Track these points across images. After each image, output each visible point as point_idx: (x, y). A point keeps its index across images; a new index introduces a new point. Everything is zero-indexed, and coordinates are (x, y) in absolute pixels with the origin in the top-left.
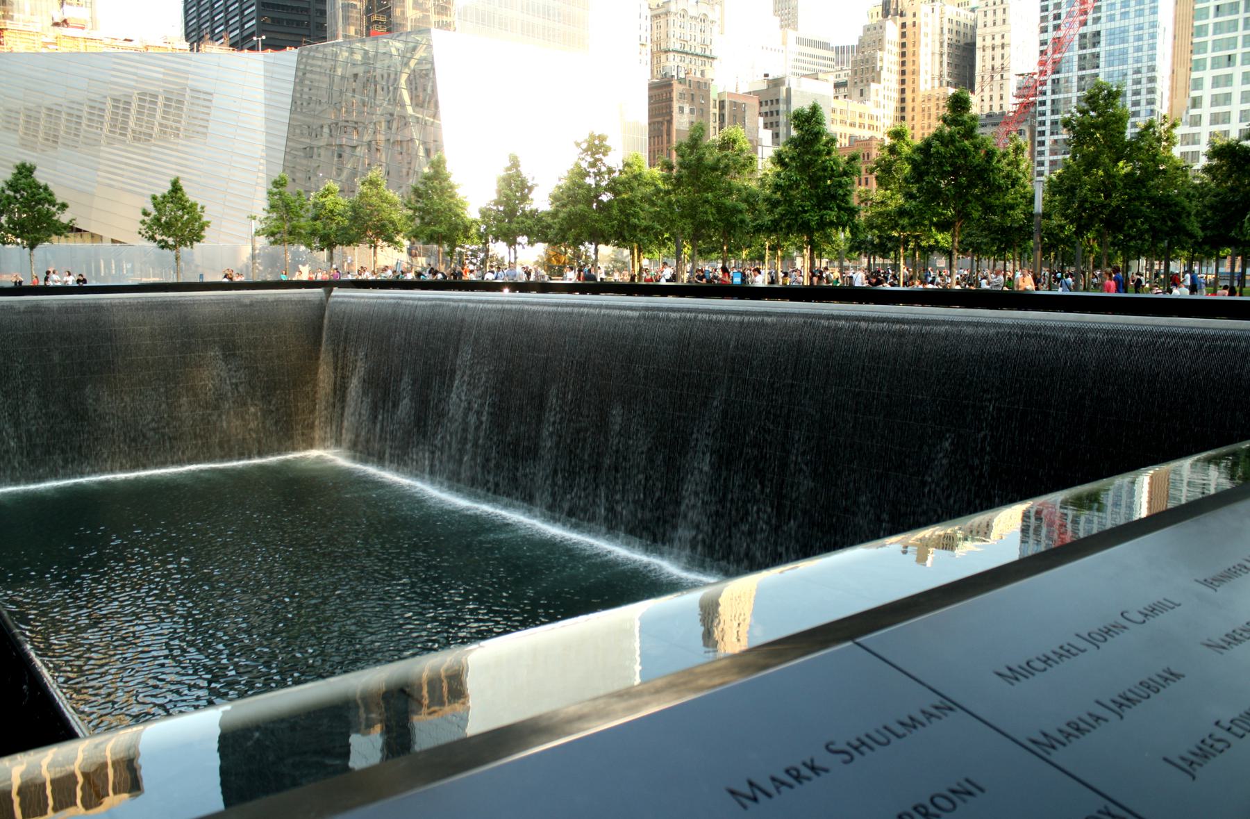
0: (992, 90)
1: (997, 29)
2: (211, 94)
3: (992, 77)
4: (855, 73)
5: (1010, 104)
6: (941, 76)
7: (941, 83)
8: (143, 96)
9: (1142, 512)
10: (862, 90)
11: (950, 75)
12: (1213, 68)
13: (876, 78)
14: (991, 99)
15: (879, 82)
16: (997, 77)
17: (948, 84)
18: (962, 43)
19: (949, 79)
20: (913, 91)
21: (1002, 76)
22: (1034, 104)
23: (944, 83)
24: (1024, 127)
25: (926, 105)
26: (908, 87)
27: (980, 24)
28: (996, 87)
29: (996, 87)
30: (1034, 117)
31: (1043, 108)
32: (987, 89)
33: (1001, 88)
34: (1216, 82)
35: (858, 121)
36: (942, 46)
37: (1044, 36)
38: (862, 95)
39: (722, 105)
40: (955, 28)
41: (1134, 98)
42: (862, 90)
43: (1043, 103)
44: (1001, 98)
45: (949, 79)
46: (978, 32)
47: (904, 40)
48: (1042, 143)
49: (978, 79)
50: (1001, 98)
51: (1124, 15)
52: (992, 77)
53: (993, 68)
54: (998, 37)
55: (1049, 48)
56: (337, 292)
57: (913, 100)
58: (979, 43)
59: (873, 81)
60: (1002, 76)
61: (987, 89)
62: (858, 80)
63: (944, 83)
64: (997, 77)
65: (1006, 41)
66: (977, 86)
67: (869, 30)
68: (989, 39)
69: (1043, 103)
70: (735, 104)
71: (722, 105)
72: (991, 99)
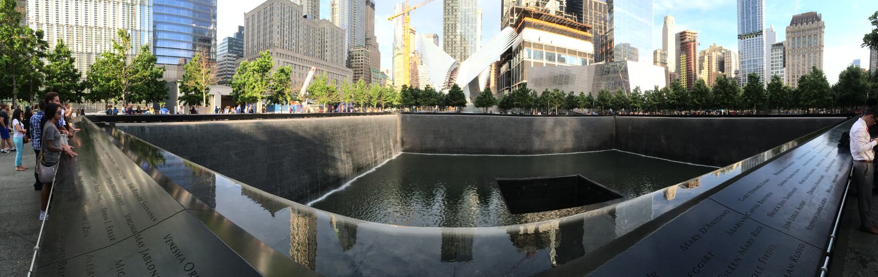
9: (766, 160)
13: (703, 69)
39: (671, 75)
51: (756, 57)
70: (673, 75)
71: (671, 75)
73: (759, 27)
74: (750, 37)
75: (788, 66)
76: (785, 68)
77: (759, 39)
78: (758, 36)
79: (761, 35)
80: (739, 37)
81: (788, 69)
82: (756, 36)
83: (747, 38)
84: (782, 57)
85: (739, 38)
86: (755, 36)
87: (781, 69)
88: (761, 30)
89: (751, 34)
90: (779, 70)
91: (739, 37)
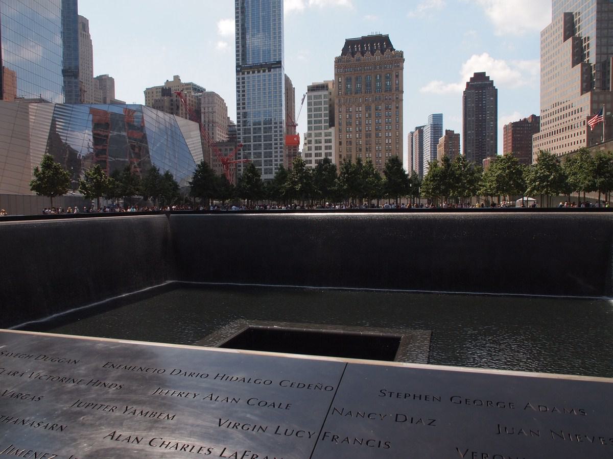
1: (210, 105)
3: (208, 125)
12: (314, 130)
16: (211, 125)
18: (194, 109)
21: (213, 125)
22: (236, 138)
24: (233, 147)
27: (202, 101)
28: (210, 129)
30: (236, 143)
33: (213, 129)
34: (316, 135)
36: (186, 110)
37: (239, 111)
40: (191, 103)
44: (213, 133)
46: (202, 106)
47: (172, 107)
48: (240, 154)
51: (270, 106)
52: (208, 125)
53: (209, 122)
54: (210, 109)
55: (241, 116)
58: (203, 110)
64: (211, 125)
65: (214, 110)
67: (157, 101)
68: (206, 109)
73: (275, 55)
74: (259, 72)
75: (340, 124)
76: (333, 128)
77: (275, 75)
78: (272, 70)
79: (278, 69)
80: (239, 69)
81: (340, 131)
82: (269, 71)
83: (254, 72)
84: (328, 109)
85: (237, 72)
86: (267, 71)
87: (326, 128)
88: (277, 60)
89: (261, 66)
90: (323, 132)
91: (239, 69)
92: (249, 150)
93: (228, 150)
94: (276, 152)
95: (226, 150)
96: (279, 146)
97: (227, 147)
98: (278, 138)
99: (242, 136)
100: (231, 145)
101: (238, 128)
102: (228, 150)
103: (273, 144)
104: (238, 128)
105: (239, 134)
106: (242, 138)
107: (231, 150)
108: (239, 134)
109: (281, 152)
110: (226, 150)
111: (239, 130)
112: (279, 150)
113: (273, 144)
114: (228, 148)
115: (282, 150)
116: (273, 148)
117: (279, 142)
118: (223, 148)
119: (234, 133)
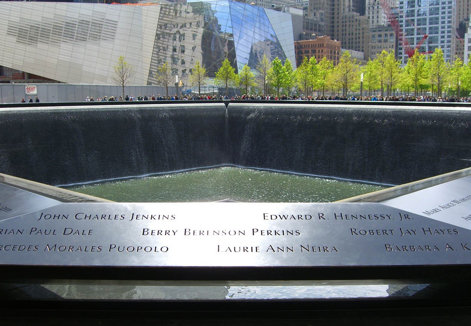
0: (373, 13)
2: (117, 22)
4: (311, 4)
5: (384, 20)
6: (349, 6)
7: (349, 10)
8: (82, 22)
10: (315, 13)
11: (353, 6)
14: (373, 17)
15: (323, 10)
16: (376, 7)
17: (353, 10)
19: (353, 8)
20: (338, 14)
21: (378, 7)
23: (351, 10)
24: (394, 32)
25: (344, 20)
26: (336, 11)
28: (375, 12)
29: (375, 12)
31: (402, 23)
32: (371, 13)
33: (378, 12)
35: (313, 27)
38: (315, 15)
41: (442, 20)
42: (315, 13)
43: (402, 21)
44: (378, 17)
45: (353, 8)
49: (367, 8)
50: (378, 17)
56: (230, 104)
57: (338, 18)
59: (320, 9)
60: (378, 7)
61: (371, 13)
62: (312, 8)
63: (351, 10)
64: (376, 7)
66: (367, 12)
69: (402, 21)
72: (373, 17)
92: (412, 35)
93: (389, 35)
94: (443, 37)
95: (386, 35)
96: (446, 30)
97: (387, 32)
98: (446, 20)
99: (404, 19)
100: (392, 30)
101: (401, 10)
102: (389, 35)
103: (440, 28)
104: (401, 10)
105: (401, 17)
106: (404, 21)
107: (391, 35)
108: (401, 17)
109: (449, 37)
110: (386, 35)
111: (401, 12)
112: (446, 35)
113: (440, 28)
114: (388, 33)
115: (450, 34)
116: (440, 32)
117: (446, 25)
118: (383, 33)
119: (396, 16)
